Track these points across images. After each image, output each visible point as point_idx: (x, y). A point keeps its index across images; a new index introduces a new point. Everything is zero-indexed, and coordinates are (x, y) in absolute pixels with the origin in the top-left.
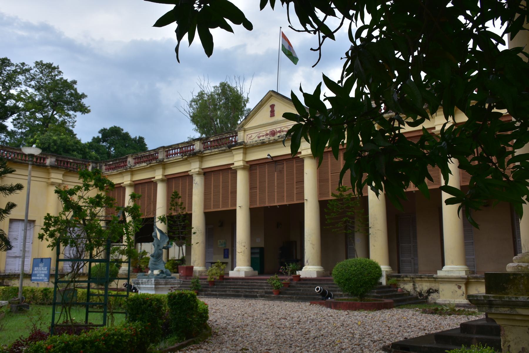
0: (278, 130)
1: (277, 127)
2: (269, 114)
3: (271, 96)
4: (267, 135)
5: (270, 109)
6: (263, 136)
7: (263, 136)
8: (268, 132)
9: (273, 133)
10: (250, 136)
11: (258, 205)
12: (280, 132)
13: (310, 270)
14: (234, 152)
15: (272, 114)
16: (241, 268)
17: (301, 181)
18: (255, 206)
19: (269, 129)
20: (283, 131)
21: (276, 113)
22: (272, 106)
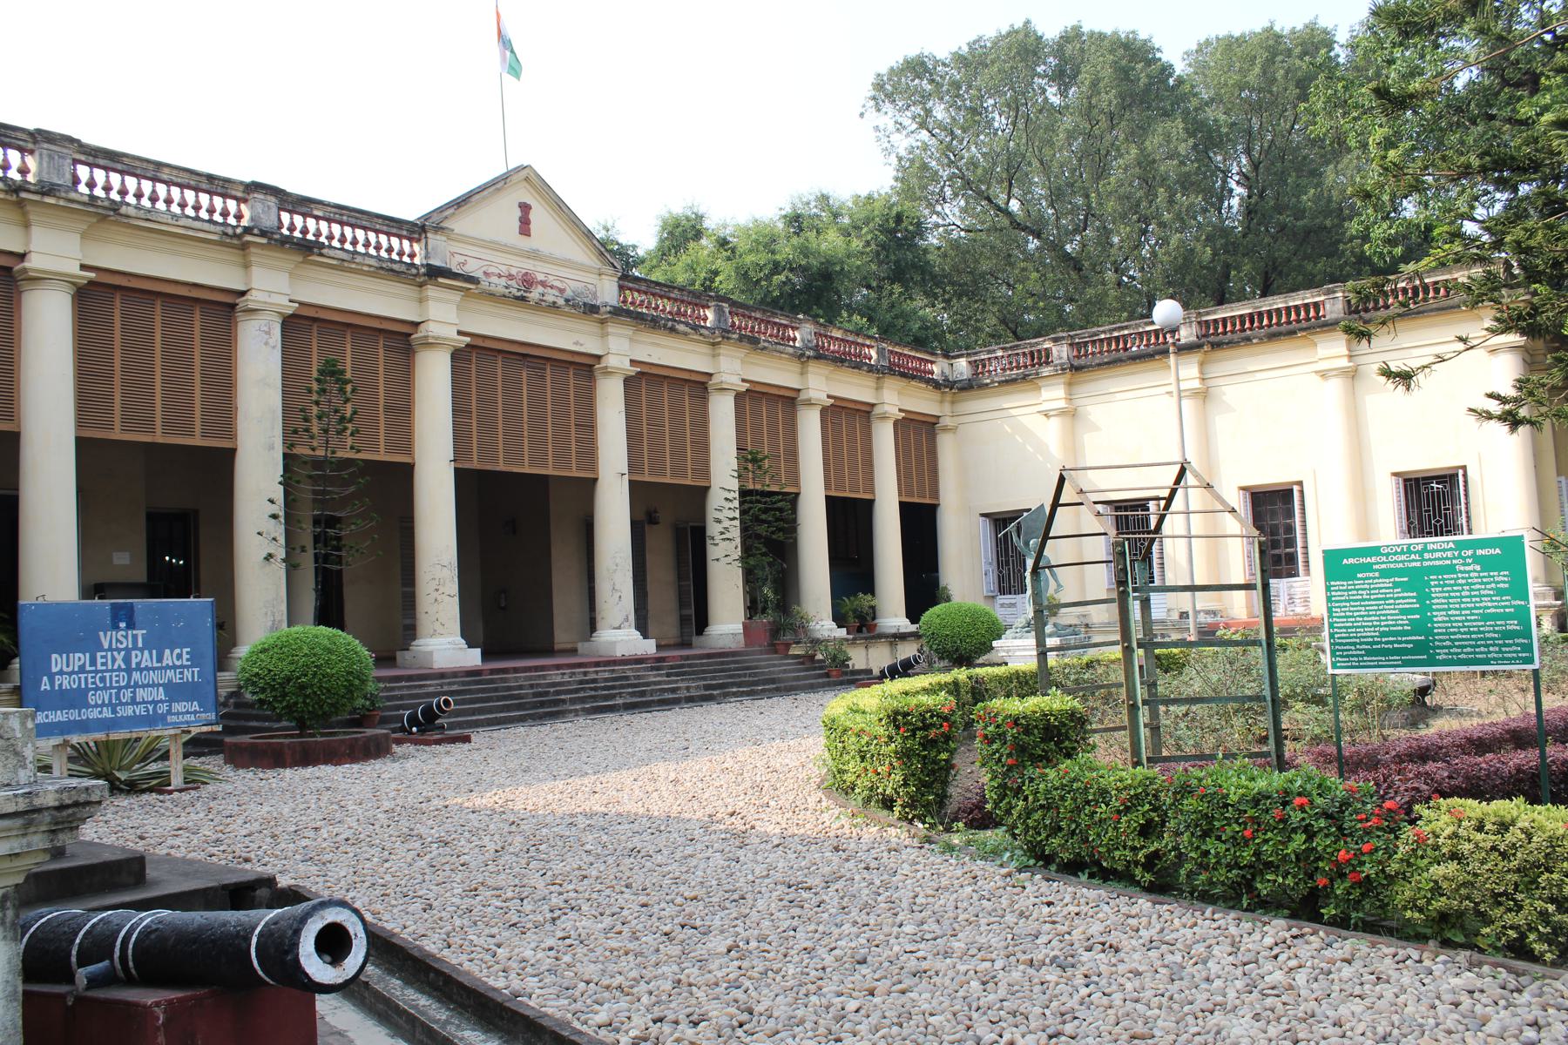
0: (540, 277)
1: (540, 271)
2: (517, 224)
3: (527, 179)
4: (510, 277)
5: (518, 213)
6: (500, 276)
7: (500, 276)
8: (514, 271)
9: (528, 281)
10: (462, 259)
11: (475, 464)
12: (543, 284)
13: (620, 636)
14: (431, 291)
15: (525, 227)
16: (444, 644)
17: (588, 426)
18: (467, 466)
19: (519, 265)
20: (552, 287)
21: (532, 226)
22: (525, 208)
